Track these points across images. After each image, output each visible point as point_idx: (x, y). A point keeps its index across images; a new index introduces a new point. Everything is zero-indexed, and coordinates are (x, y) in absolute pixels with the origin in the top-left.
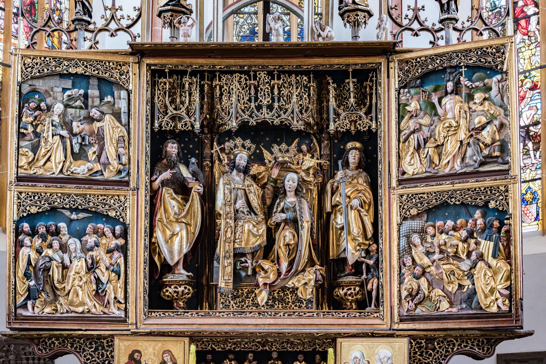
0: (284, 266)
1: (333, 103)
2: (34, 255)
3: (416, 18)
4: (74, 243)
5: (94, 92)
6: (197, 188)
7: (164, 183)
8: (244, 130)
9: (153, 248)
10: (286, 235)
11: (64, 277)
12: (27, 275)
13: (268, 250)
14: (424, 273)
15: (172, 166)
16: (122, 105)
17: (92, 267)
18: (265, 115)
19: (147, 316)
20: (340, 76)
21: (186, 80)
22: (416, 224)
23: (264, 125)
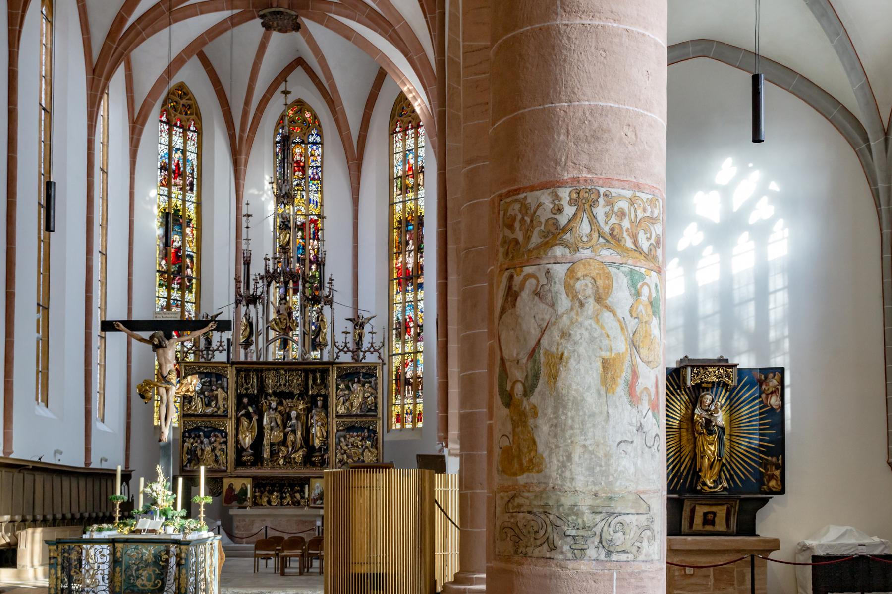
0: (290, 449)
1: (310, 382)
2: (190, 446)
3: (346, 346)
4: (206, 440)
5: (214, 379)
6: (255, 418)
7: (242, 415)
8: (275, 393)
9: (237, 441)
10: (291, 437)
11: (202, 454)
12: (187, 454)
13: (284, 443)
14: (345, 453)
15: (246, 408)
16: (226, 385)
17: (213, 450)
18: (283, 388)
19: (236, 469)
20: (314, 372)
21: (251, 374)
22: (342, 433)
23: (282, 392)
